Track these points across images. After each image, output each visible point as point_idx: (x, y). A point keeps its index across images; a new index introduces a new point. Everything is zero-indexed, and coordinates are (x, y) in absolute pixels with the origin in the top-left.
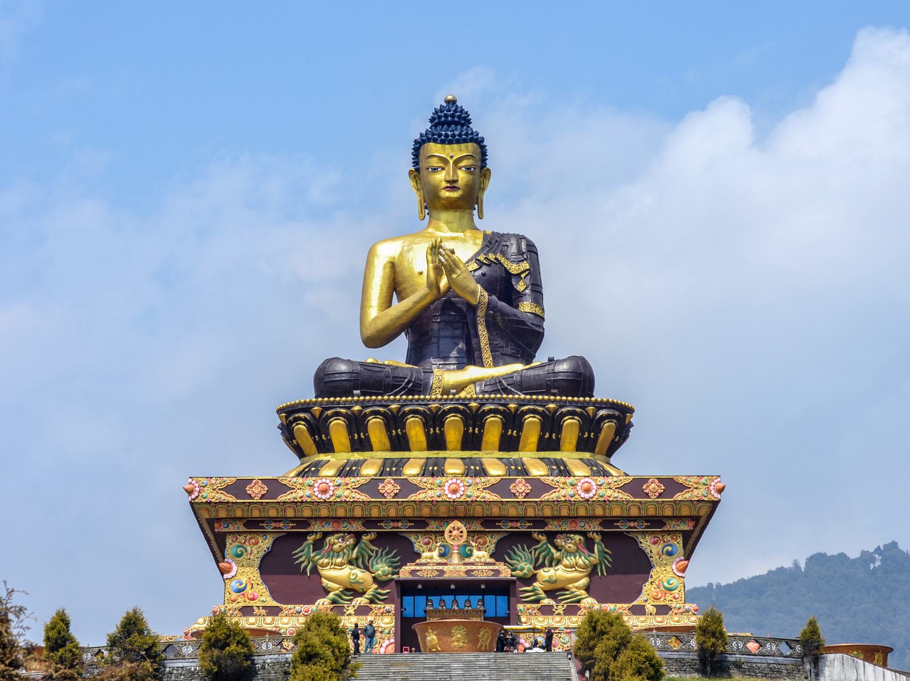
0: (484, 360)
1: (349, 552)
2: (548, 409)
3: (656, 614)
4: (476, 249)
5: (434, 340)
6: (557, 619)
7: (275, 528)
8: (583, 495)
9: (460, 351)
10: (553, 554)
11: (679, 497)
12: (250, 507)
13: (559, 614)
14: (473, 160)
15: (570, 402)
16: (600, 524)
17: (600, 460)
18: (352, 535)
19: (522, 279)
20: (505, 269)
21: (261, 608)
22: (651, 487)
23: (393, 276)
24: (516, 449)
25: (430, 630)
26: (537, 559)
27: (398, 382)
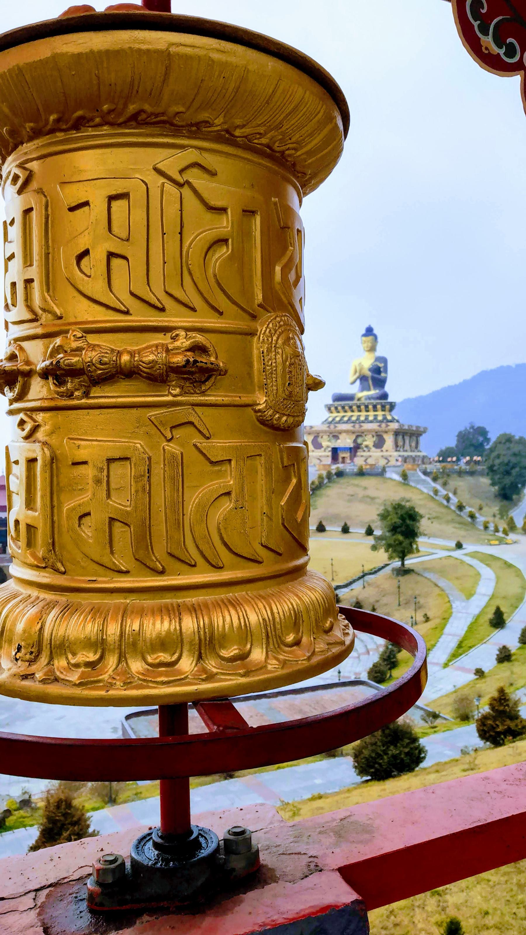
17: (387, 413)
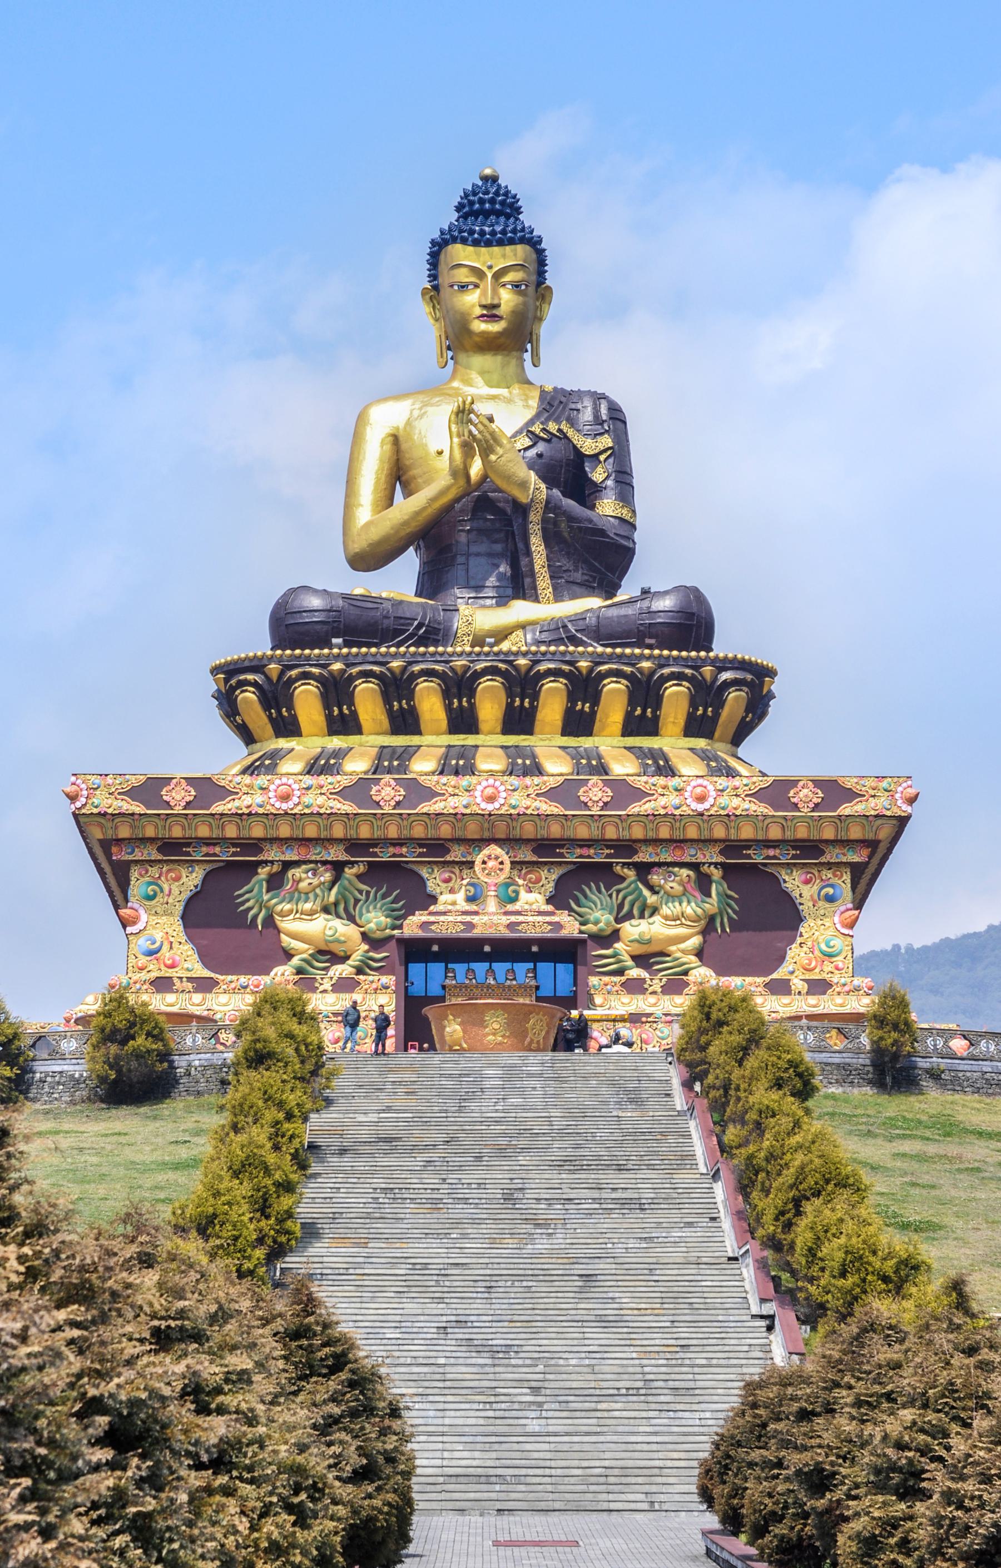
0: (539, 592)
1: (323, 892)
3: (808, 993)
4: (529, 414)
5: (460, 559)
6: (652, 999)
7: (207, 855)
8: (695, 805)
9: (501, 577)
10: (645, 899)
11: (846, 809)
12: (169, 821)
13: (654, 993)
14: (525, 271)
15: (675, 659)
16: (721, 853)
17: (721, 750)
18: (328, 866)
19: (600, 462)
20: (575, 447)
21: (184, 980)
22: (801, 794)
23: (395, 457)
24: (590, 734)
25: (451, 1017)
26: (621, 906)
27: (403, 625)
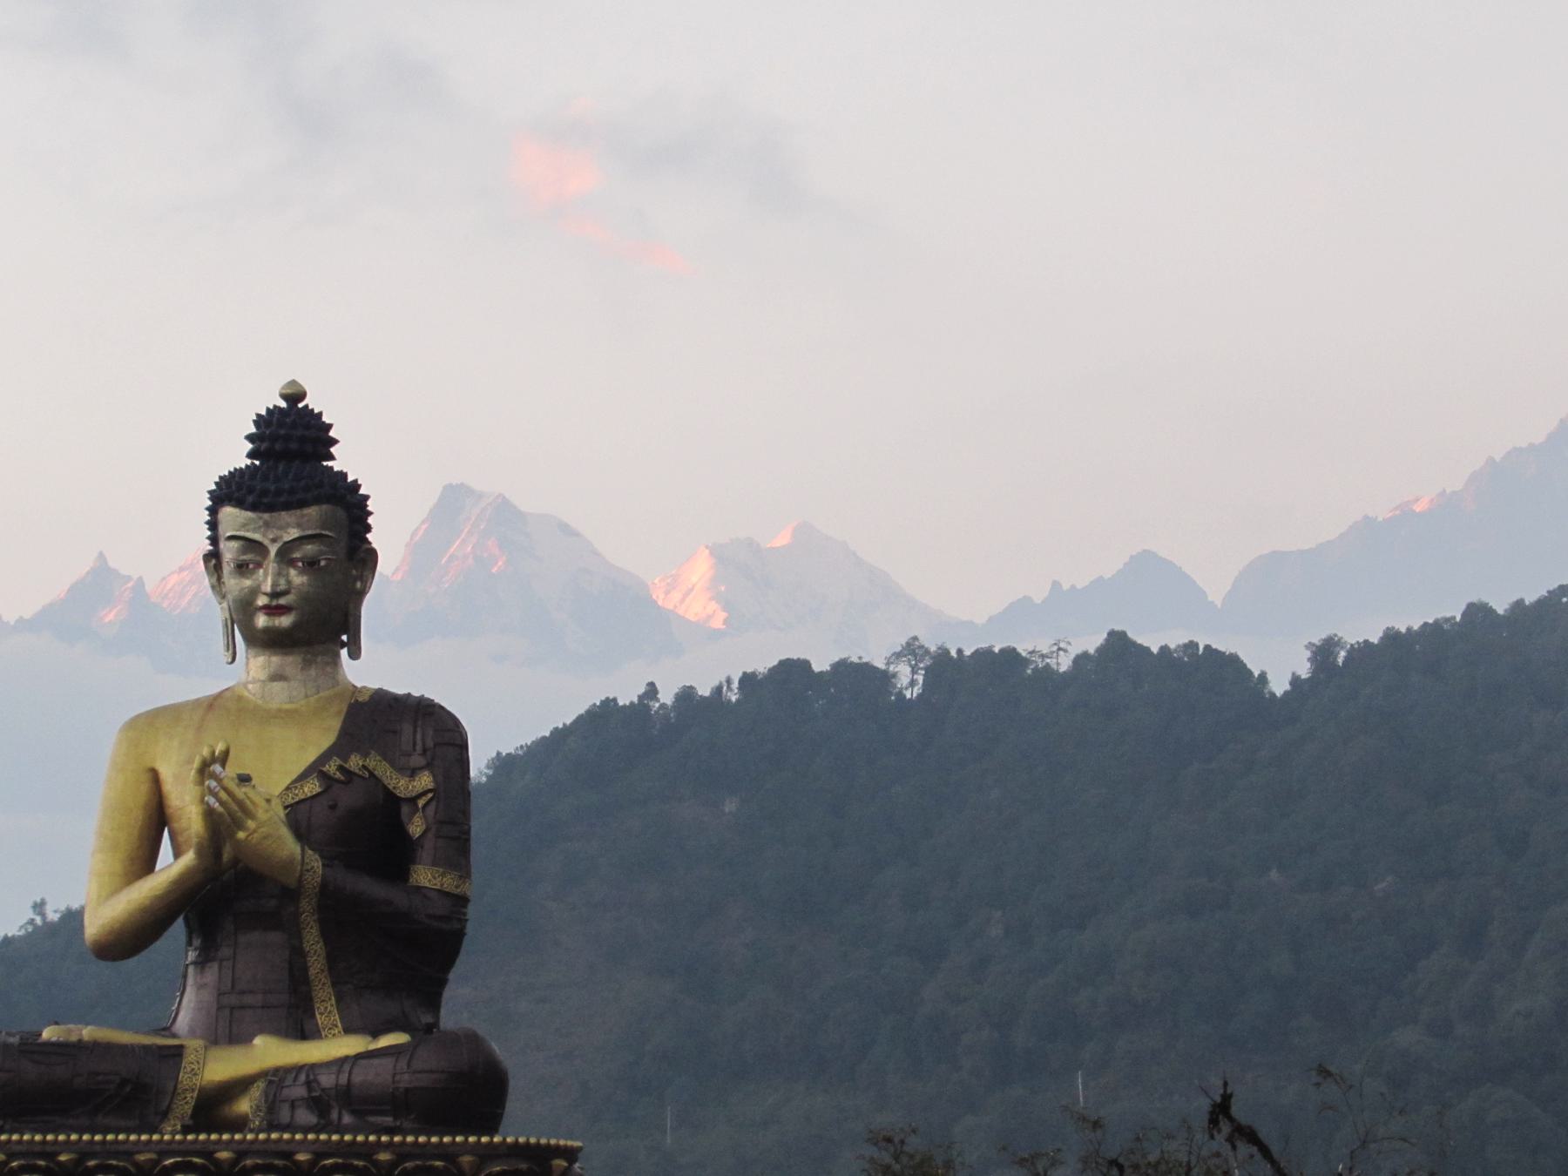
2: (376, 1163)
4: (326, 740)
20: (385, 787)
